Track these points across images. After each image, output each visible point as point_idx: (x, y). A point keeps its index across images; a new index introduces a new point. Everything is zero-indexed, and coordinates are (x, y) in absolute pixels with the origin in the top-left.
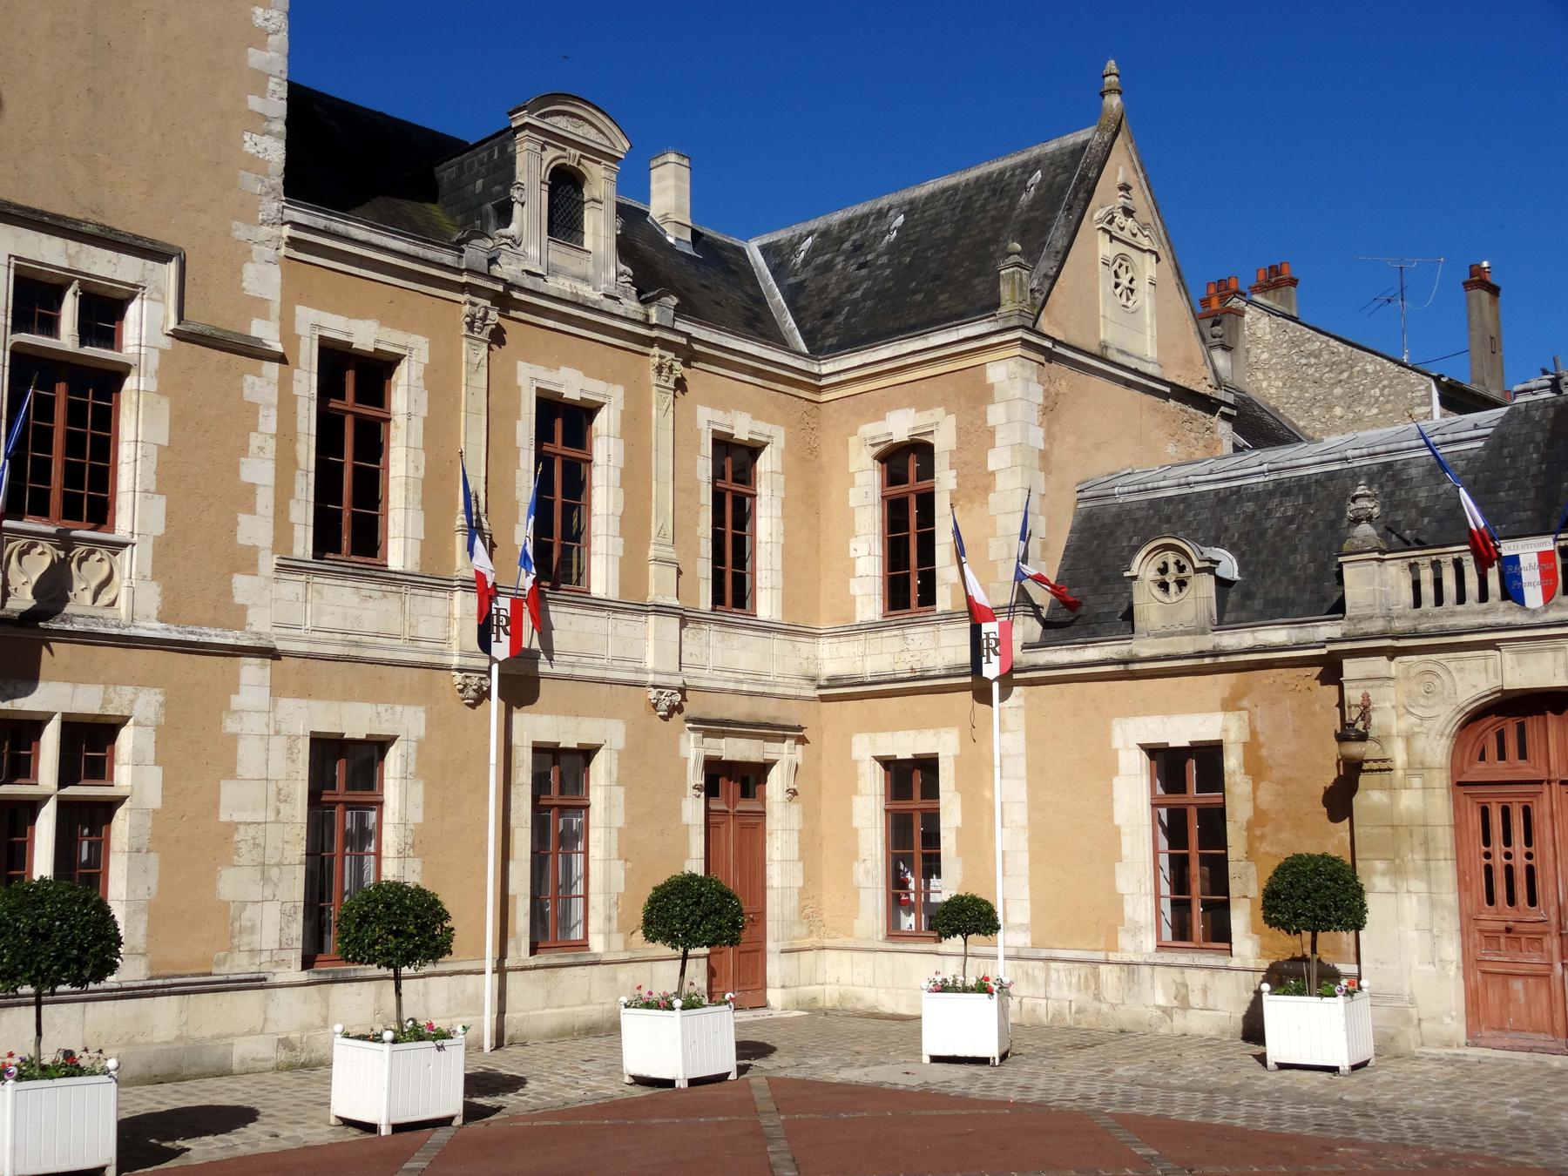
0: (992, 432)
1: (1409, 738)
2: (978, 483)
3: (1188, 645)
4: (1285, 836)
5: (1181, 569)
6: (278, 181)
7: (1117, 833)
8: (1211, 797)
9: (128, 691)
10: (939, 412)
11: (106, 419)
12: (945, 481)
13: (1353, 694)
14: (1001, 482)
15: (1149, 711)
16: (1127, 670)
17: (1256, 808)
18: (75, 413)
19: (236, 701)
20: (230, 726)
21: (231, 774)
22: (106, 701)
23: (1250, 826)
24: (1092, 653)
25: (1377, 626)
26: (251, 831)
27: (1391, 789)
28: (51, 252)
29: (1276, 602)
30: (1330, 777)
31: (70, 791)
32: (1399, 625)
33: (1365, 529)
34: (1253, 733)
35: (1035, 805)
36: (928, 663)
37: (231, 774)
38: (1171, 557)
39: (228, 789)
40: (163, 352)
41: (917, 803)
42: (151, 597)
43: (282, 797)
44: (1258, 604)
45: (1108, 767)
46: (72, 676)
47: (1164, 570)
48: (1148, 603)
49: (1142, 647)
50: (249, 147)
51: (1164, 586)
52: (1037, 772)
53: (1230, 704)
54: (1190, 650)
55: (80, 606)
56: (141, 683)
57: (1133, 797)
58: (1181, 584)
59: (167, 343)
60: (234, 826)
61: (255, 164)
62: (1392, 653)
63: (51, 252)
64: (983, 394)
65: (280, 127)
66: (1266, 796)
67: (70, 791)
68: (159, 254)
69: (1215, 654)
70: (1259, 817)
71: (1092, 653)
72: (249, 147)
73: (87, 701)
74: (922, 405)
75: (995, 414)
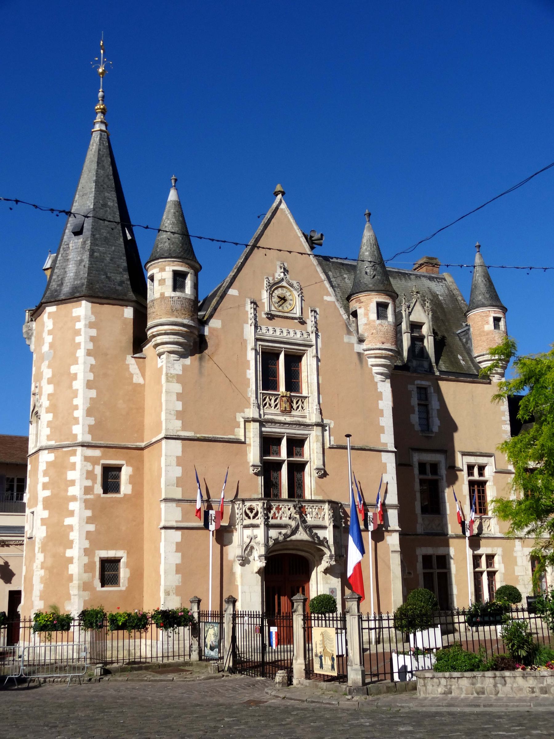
6: (509, 434)
9: (496, 548)
11: (484, 491)
18: (479, 491)
19: (515, 549)
20: (515, 554)
21: (516, 565)
22: (492, 551)
26: (522, 577)
28: (472, 460)
31: (488, 569)
37: (516, 565)
39: (516, 568)
40: (493, 476)
42: (497, 528)
43: (526, 570)
46: (487, 546)
50: (503, 428)
55: (485, 530)
56: (498, 546)
59: (494, 474)
60: (518, 576)
61: (505, 432)
63: (472, 460)
65: (509, 422)
67: (488, 569)
68: (490, 456)
72: (503, 428)
73: (489, 551)
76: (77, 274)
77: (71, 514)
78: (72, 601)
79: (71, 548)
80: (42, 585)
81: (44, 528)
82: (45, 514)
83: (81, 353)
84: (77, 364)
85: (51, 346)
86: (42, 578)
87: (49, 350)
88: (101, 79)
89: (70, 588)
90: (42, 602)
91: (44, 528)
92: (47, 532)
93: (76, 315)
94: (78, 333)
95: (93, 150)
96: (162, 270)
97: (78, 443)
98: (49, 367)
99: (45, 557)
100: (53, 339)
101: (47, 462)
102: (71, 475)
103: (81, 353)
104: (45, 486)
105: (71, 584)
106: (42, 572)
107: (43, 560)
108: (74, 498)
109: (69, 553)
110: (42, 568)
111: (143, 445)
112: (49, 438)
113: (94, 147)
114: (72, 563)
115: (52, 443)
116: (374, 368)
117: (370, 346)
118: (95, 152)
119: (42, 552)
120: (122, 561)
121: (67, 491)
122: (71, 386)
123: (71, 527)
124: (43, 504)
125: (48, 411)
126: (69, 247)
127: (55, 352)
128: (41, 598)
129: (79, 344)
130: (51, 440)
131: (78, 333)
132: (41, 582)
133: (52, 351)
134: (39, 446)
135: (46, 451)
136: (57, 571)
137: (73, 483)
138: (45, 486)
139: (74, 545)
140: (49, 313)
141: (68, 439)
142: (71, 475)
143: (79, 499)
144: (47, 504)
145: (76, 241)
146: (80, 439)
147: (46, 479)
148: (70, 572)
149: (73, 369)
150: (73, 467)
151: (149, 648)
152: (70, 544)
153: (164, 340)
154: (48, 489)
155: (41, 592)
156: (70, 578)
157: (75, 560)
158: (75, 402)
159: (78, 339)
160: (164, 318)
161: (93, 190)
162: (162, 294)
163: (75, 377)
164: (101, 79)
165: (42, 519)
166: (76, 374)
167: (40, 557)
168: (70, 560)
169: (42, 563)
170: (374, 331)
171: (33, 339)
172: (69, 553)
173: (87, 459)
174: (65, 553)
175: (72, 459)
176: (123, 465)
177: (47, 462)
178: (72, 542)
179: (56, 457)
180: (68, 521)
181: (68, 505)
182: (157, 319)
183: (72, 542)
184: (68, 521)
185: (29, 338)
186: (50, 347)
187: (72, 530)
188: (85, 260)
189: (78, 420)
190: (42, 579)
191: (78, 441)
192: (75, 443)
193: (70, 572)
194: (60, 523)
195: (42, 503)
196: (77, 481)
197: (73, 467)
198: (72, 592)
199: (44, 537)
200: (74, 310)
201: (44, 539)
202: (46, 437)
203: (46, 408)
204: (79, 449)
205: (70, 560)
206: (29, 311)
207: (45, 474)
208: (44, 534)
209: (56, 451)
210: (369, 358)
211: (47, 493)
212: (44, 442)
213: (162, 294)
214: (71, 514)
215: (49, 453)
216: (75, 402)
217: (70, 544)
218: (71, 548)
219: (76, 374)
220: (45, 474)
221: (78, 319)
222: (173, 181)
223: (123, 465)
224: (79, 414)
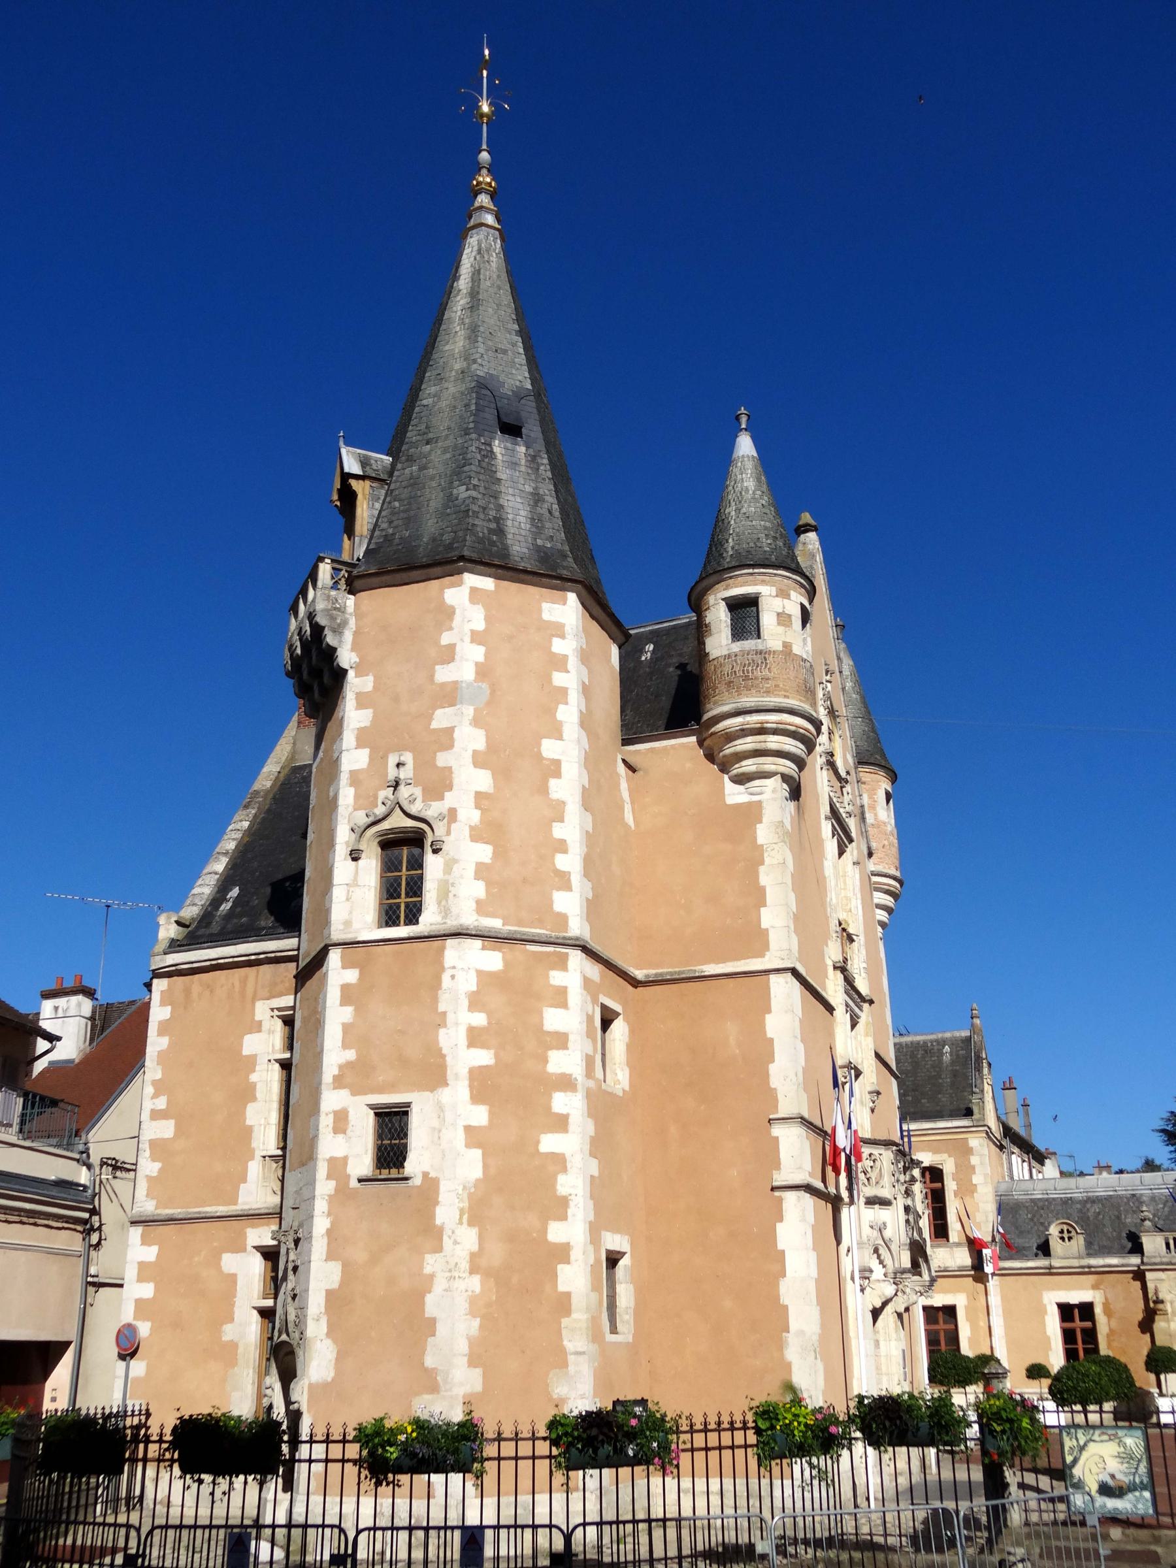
0: (973, 1168)
1: (1171, 1303)
2: (966, 1189)
3: (1075, 1263)
4: (1123, 1339)
5: (1069, 1232)
7: (1048, 1338)
8: (1088, 1324)
10: (945, 1156)
12: (950, 1186)
13: (1151, 1286)
14: (979, 1188)
15: (1059, 1288)
16: (1050, 1272)
17: (1110, 1329)
23: (1108, 1336)
24: (1031, 1264)
25: (1158, 1260)
27: (1168, 1321)
29: (1104, 1247)
30: (1140, 1316)
32: (1165, 1260)
33: (1147, 1223)
34: (1106, 1299)
35: (1008, 1327)
36: (948, 1264)
38: (1065, 1227)
41: (942, 1326)
44: (1096, 1247)
45: (1043, 1311)
47: (1062, 1232)
48: (1056, 1245)
49: (1056, 1263)
51: (1063, 1239)
52: (1007, 1314)
53: (1095, 1287)
54: (1077, 1265)
57: (1053, 1326)
58: (1070, 1238)
62: (1163, 1270)
64: (969, 1151)
66: (1114, 1324)
69: (1089, 1267)
70: (1111, 1333)
71: (1031, 1264)
74: (936, 1151)
75: (974, 1160)
76: (536, 522)
77: (561, 1123)
78: (572, 1369)
79: (563, 1217)
80: (476, 1323)
81: (477, 1153)
82: (480, 1116)
83: (569, 714)
84: (561, 738)
85: (482, 671)
86: (473, 1300)
87: (475, 681)
88: (485, 126)
89: (564, 1332)
90: (477, 1373)
91: (477, 1153)
92: (485, 1166)
93: (553, 619)
94: (560, 663)
95: (494, 265)
96: (783, 594)
97: (570, 938)
98: (476, 722)
99: (481, 1238)
100: (487, 655)
101: (480, 973)
102: (553, 1019)
103: (569, 714)
104: (475, 1038)
105: (565, 1322)
106: (475, 1283)
107: (475, 1248)
108: (566, 1083)
109: (557, 1232)
110: (472, 1272)
111: (639, 974)
112: (481, 907)
113: (494, 258)
114: (567, 1261)
115: (494, 924)
116: (879, 911)
117: (880, 868)
118: (498, 268)
119: (471, 1224)
120: (621, 1263)
121: (546, 1061)
122: (544, 790)
123: (559, 1161)
124: (471, 1087)
125: (476, 835)
126: (492, 452)
127: (493, 692)
128: (473, 1362)
129: (564, 691)
130: (493, 915)
131: (560, 663)
132: (472, 1313)
133: (485, 686)
134: (452, 924)
135: (478, 943)
136: (520, 1280)
137: (561, 1041)
138: (475, 1038)
139: (570, 1212)
140: (474, 590)
141: (541, 923)
142: (553, 1019)
143: (579, 1087)
144: (482, 1086)
145: (509, 445)
146: (577, 927)
147: (480, 1019)
148: (562, 1287)
149: (550, 748)
150: (560, 998)
151: (715, 1500)
152: (560, 1208)
153: (787, 748)
154: (484, 1046)
155: (472, 1342)
156: (564, 1304)
157: (576, 1254)
158: (558, 831)
159: (559, 679)
160: (793, 698)
161: (521, 351)
162: (787, 646)
163: (554, 769)
164: (485, 126)
165: (468, 1129)
166: (557, 763)
167: (463, 1240)
168: (562, 1253)
169: (473, 1256)
170: (886, 843)
171: (348, 636)
172: (557, 1232)
173: (587, 983)
174: (544, 1231)
175: (557, 978)
176: (618, 1014)
177: (480, 973)
178: (564, 1202)
179: (506, 963)
180: (549, 1143)
181: (550, 1097)
182: (778, 696)
183: (564, 1202)
184: (549, 1143)
185: (338, 631)
186: (477, 673)
187: (564, 1170)
188: (548, 498)
189: (569, 880)
190: (475, 1306)
191: (571, 934)
192: (564, 938)
193: (562, 1287)
194: (526, 1146)
195: (467, 1083)
196: (571, 1037)
197: (560, 998)
198: (569, 1345)
199: (477, 1180)
200: (545, 606)
201: (475, 1186)
202: (474, 905)
203: (472, 828)
204: (576, 958)
205: (562, 1253)
206: (333, 561)
207: (475, 1002)
208: (477, 1172)
209: (506, 947)
210: (877, 890)
211: (484, 1057)
212: (469, 918)
213: (787, 646)
214: (561, 1123)
215: (484, 948)
216: (558, 831)
217: (560, 1208)
218: (563, 1217)
219: (557, 763)
220: (475, 1002)
221: (558, 630)
222: (744, 419)
223: (618, 1014)
224: (570, 862)
